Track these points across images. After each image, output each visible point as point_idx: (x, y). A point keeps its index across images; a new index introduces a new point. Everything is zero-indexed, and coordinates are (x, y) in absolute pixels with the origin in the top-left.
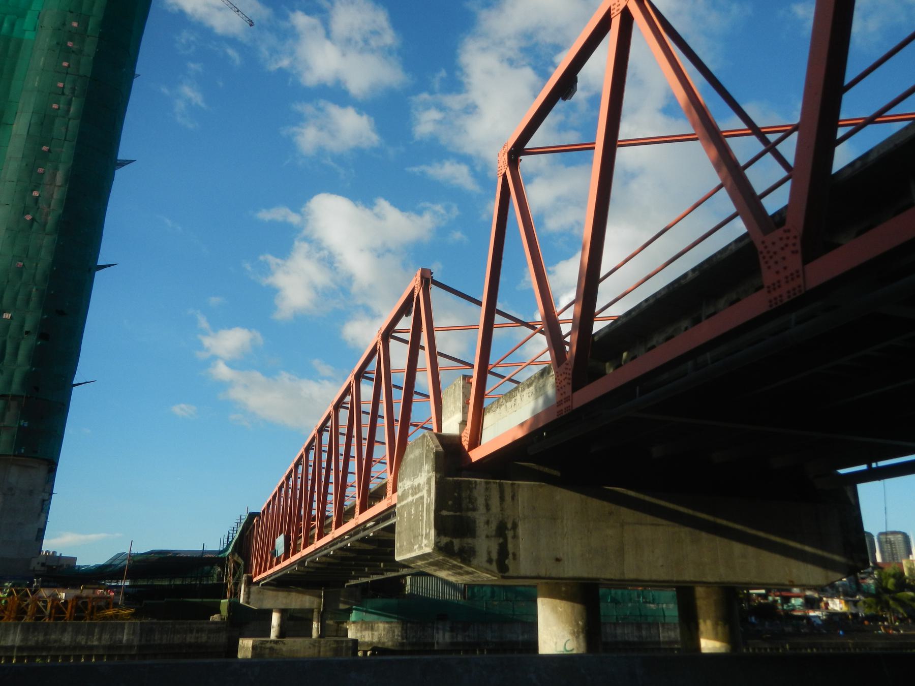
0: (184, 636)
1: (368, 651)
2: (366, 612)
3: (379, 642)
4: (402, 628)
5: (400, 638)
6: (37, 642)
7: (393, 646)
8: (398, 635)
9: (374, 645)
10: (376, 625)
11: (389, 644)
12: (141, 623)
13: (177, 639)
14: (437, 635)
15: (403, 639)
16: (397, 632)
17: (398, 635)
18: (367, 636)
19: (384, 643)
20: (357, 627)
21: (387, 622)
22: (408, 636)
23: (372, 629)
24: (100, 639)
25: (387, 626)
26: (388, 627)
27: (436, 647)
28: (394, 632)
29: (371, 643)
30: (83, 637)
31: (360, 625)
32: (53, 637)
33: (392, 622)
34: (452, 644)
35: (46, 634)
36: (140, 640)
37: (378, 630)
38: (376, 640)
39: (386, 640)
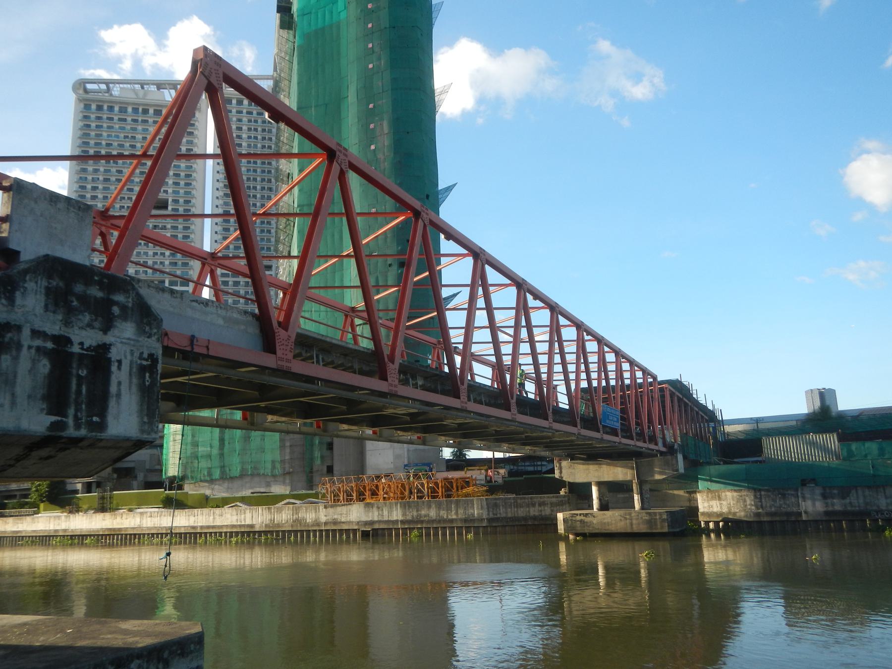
0: (528, 509)
1: (710, 522)
2: (711, 481)
3: (730, 513)
4: (755, 497)
5: (753, 508)
6: (413, 516)
7: (746, 516)
8: (751, 505)
9: (724, 516)
11: (741, 515)
12: (486, 499)
13: (521, 512)
14: (803, 503)
15: (757, 508)
16: (750, 499)
18: (715, 506)
19: (735, 514)
20: (702, 497)
21: (735, 491)
22: (764, 505)
23: (720, 499)
26: (739, 496)
29: (721, 514)
31: (705, 494)
32: (423, 512)
33: (741, 490)
37: (726, 499)
38: (725, 510)
39: (738, 511)
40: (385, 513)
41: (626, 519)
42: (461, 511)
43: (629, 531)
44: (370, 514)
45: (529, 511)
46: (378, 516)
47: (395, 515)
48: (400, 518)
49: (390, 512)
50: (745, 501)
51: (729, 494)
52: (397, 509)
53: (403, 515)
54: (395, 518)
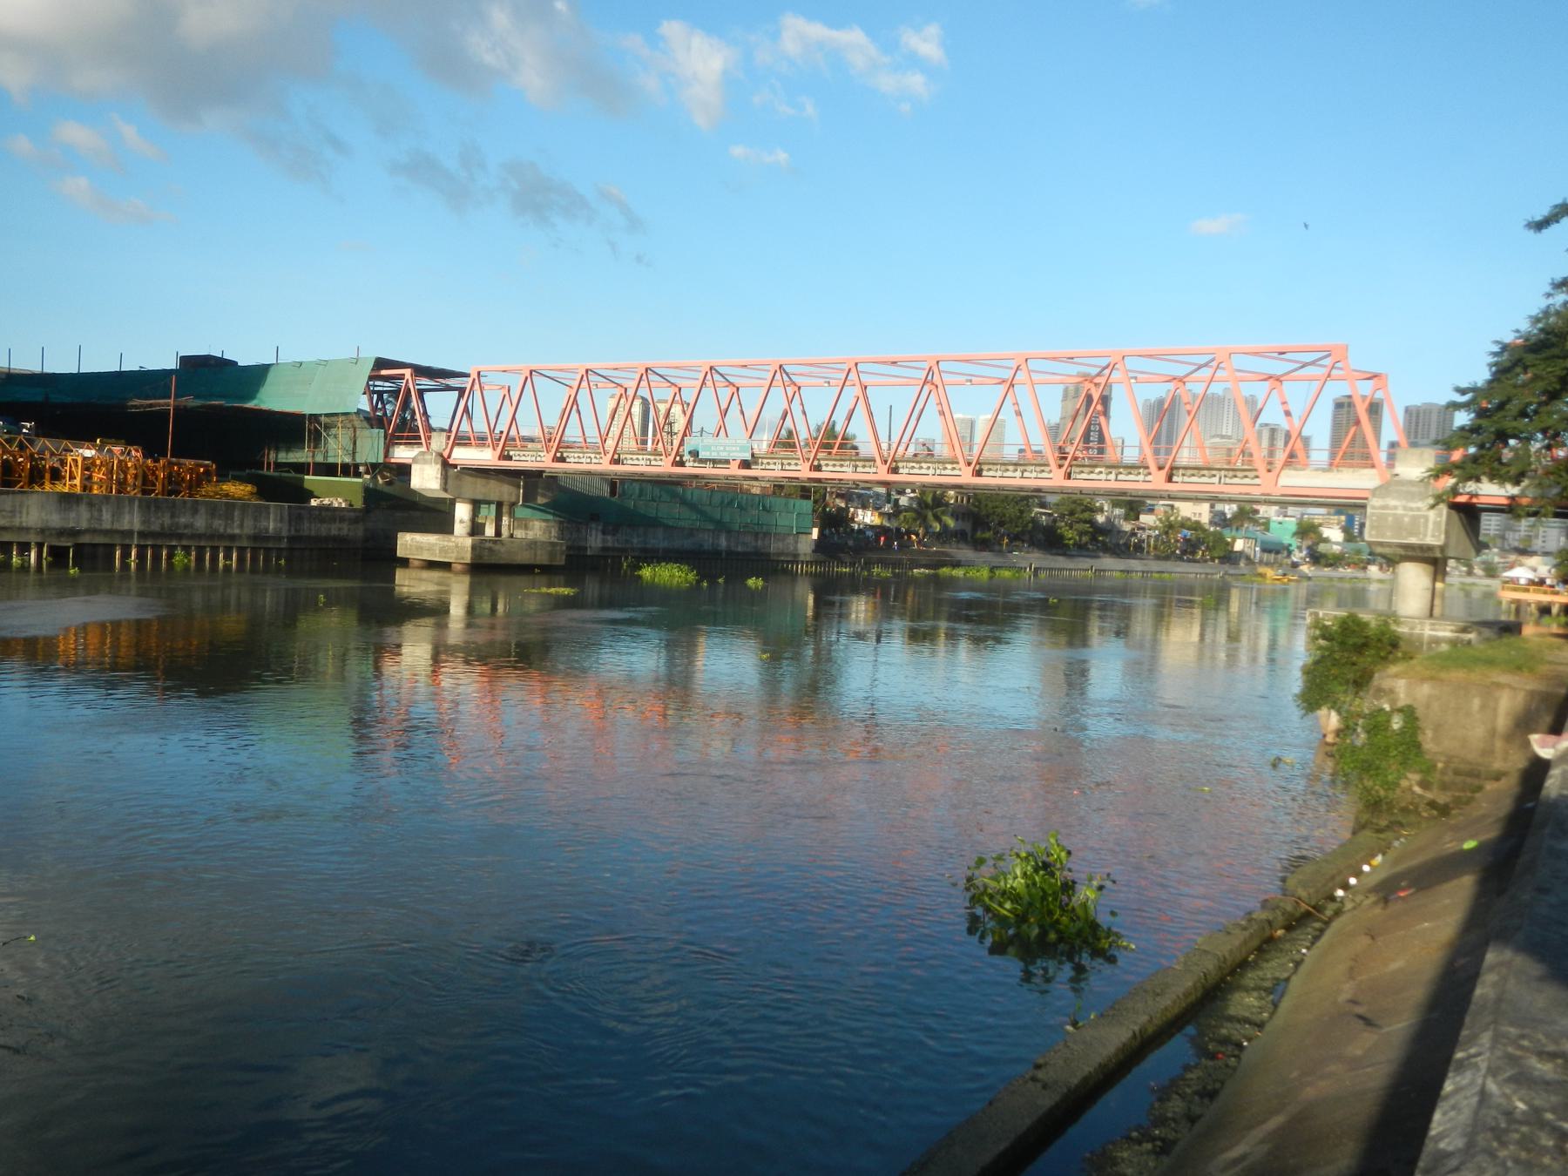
6: (162, 525)
21: (545, 521)
23: (526, 528)
24: (241, 526)
32: (183, 520)
34: (604, 549)
36: (289, 530)
37: (532, 529)
43: (532, 562)
44: (73, 515)
45: (330, 529)
46: (89, 520)
50: (550, 533)
51: (537, 524)
52: (131, 512)
53: (143, 522)
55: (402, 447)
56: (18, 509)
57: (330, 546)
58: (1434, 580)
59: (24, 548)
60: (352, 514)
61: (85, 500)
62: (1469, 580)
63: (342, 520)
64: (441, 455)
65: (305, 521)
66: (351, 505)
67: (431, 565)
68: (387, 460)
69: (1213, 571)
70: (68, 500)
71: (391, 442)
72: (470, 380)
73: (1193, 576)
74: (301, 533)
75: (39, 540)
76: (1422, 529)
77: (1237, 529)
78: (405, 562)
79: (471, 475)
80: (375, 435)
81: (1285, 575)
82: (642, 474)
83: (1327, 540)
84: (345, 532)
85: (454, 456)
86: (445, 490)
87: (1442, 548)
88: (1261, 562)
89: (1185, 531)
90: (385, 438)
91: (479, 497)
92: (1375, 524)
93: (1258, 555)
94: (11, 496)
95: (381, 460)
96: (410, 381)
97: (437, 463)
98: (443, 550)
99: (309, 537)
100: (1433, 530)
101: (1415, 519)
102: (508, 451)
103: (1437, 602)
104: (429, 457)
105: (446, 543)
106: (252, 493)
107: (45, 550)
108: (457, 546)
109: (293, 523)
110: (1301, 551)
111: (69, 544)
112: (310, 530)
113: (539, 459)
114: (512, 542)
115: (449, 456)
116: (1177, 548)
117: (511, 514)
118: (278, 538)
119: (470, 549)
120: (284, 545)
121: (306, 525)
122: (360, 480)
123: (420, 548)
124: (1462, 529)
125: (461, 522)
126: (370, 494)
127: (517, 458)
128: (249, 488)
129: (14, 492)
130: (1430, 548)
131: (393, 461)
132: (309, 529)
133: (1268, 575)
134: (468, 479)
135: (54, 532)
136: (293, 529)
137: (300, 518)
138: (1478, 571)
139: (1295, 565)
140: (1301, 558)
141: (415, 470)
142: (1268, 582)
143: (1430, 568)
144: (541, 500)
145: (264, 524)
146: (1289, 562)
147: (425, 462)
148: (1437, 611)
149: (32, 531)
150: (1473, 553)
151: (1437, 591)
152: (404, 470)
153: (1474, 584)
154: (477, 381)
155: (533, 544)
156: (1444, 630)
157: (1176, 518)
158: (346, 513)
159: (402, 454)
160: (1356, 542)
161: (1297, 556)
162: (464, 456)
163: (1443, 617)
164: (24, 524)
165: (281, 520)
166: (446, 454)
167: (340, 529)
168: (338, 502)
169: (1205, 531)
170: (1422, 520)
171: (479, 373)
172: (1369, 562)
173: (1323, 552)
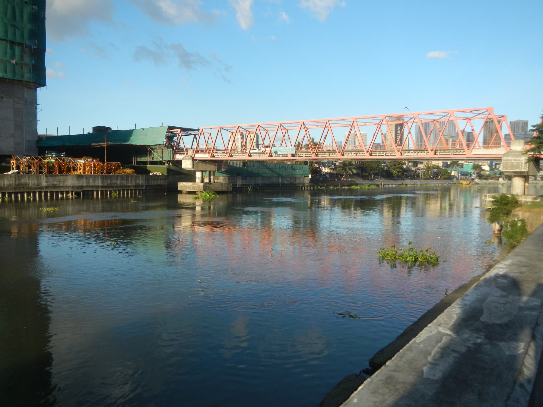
10: (219, 177)
17: (227, 182)
24: (131, 183)
25: (223, 177)
27: (238, 186)
28: (225, 180)
30: (125, 182)
35: (111, 181)
36: (145, 183)
40: (91, 181)
41: (221, 186)
42: (133, 181)
44: (81, 182)
45: (157, 182)
46: (86, 183)
47: (97, 183)
48: (100, 184)
49: (94, 181)
54: (97, 185)
55: (178, 154)
56: (65, 181)
57: (158, 188)
58: (525, 183)
59: (68, 192)
60: (164, 177)
61: (85, 177)
62: (536, 182)
63: (161, 179)
64: (192, 157)
65: (150, 180)
66: (163, 174)
67: (190, 193)
68: (174, 159)
69: (444, 183)
70: (79, 176)
71: (175, 153)
72: (200, 132)
73: (437, 185)
74: (149, 184)
75: (72, 190)
76: (520, 167)
77: (452, 168)
78: (181, 192)
79: (201, 163)
80: (169, 151)
81: (470, 183)
82: (256, 160)
83: (484, 170)
84: (162, 183)
85: (195, 157)
86: (193, 168)
87: (527, 172)
88: (461, 179)
89: (434, 169)
90: (173, 152)
91: (204, 170)
92: (505, 165)
93: (460, 176)
94: (63, 176)
95: (172, 159)
96: (180, 133)
97: (190, 159)
98: (194, 187)
99: (151, 185)
100: (524, 167)
101: (517, 162)
102: (213, 154)
103: (526, 190)
104: (187, 157)
105: (194, 185)
106: (133, 172)
107: (74, 193)
108: (198, 186)
109: (147, 181)
110: (475, 175)
111: (81, 191)
112: (151, 183)
113: (224, 156)
114: (215, 184)
115: (194, 157)
116: (431, 175)
117: (214, 175)
118: (143, 186)
119: (202, 187)
120: (144, 188)
121: (150, 182)
122: (166, 166)
123: (186, 187)
124: (533, 165)
125: (198, 178)
126: (169, 170)
127: (216, 156)
128: (132, 170)
129: (64, 175)
130: (523, 172)
131: (175, 159)
132: (151, 183)
133: (464, 183)
134: (200, 164)
135: (76, 187)
136: (146, 183)
137: (148, 179)
138: (538, 178)
139: (473, 179)
140: (475, 177)
141: (183, 162)
142: (464, 186)
143: (523, 179)
144: (223, 170)
145: (138, 181)
146: (471, 178)
147: (186, 159)
148: (526, 193)
149: (70, 187)
150: (538, 172)
151: (526, 186)
152: (179, 162)
153: (537, 183)
154: (202, 132)
155: (221, 184)
156: (529, 199)
157: (431, 165)
158: (162, 177)
159: (178, 157)
160: (494, 170)
161: (473, 176)
162: (199, 156)
163: (528, 195)
164: (67, 185)
165: (143, 180)
166: (193, 156)
167: (160, 182)
168: (159, 174)
169: (441, 169)
170: (520, 164)
171: (203, 129)
172: (499, 177)
173: (483, 174)
